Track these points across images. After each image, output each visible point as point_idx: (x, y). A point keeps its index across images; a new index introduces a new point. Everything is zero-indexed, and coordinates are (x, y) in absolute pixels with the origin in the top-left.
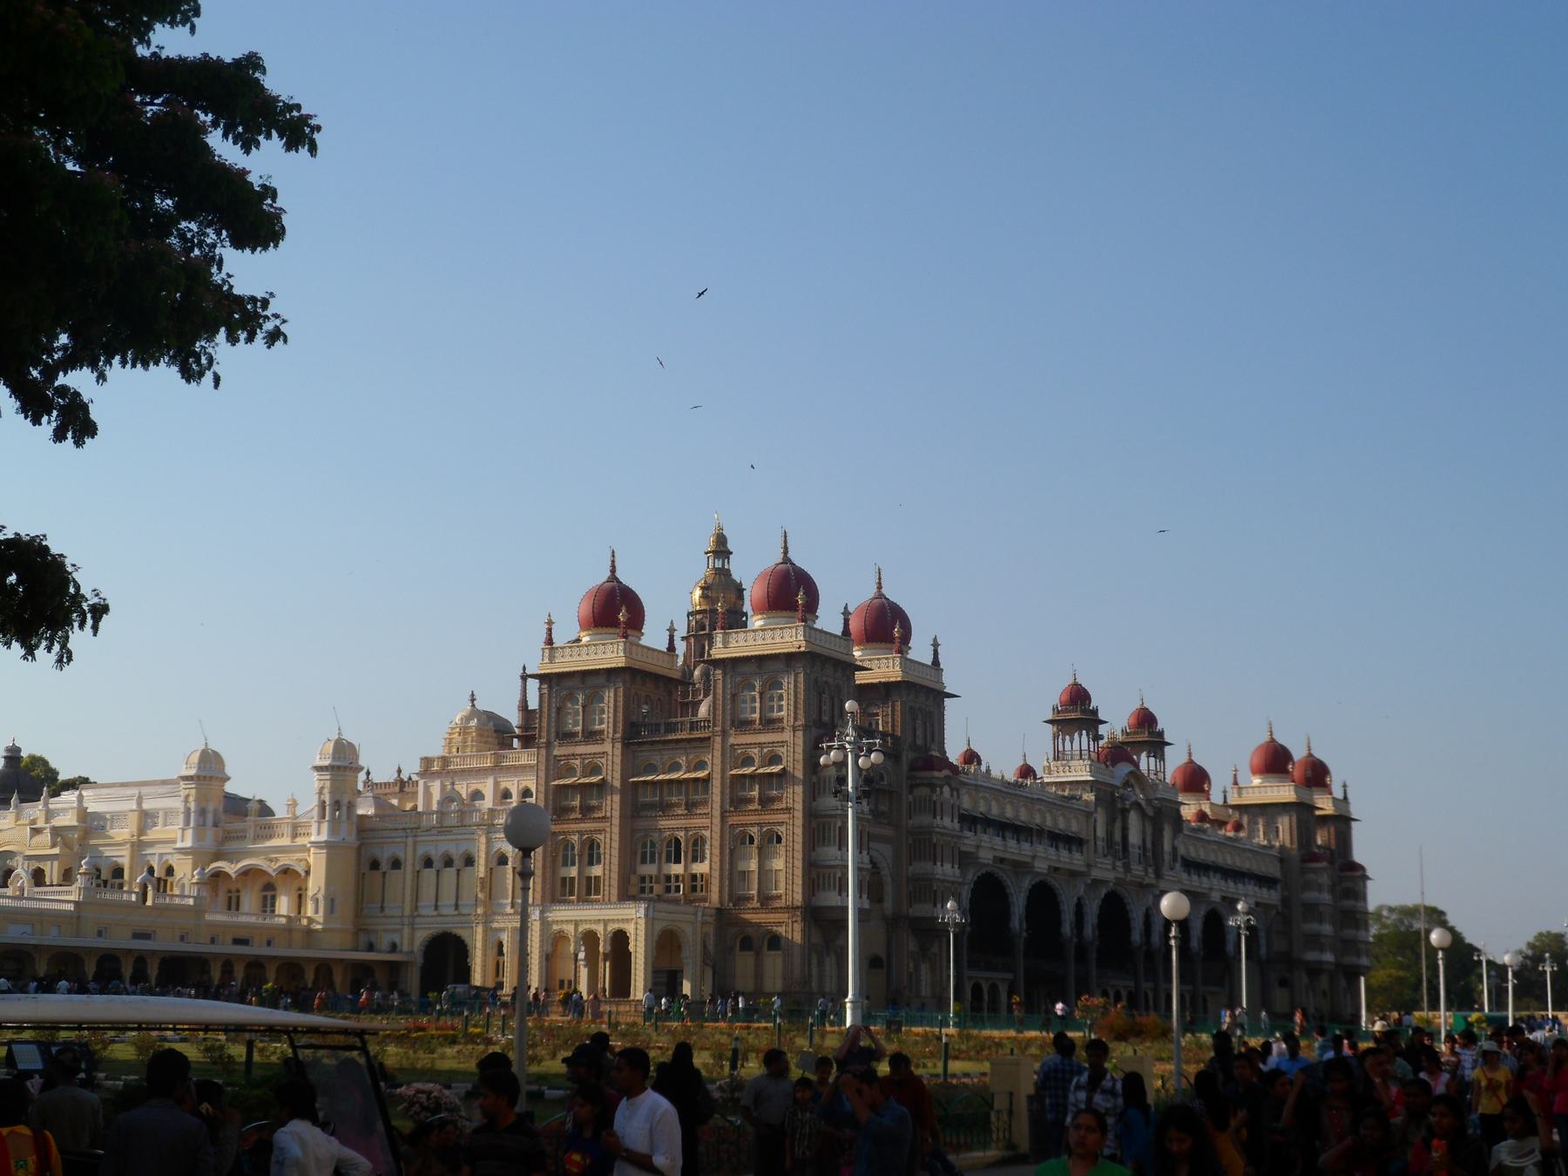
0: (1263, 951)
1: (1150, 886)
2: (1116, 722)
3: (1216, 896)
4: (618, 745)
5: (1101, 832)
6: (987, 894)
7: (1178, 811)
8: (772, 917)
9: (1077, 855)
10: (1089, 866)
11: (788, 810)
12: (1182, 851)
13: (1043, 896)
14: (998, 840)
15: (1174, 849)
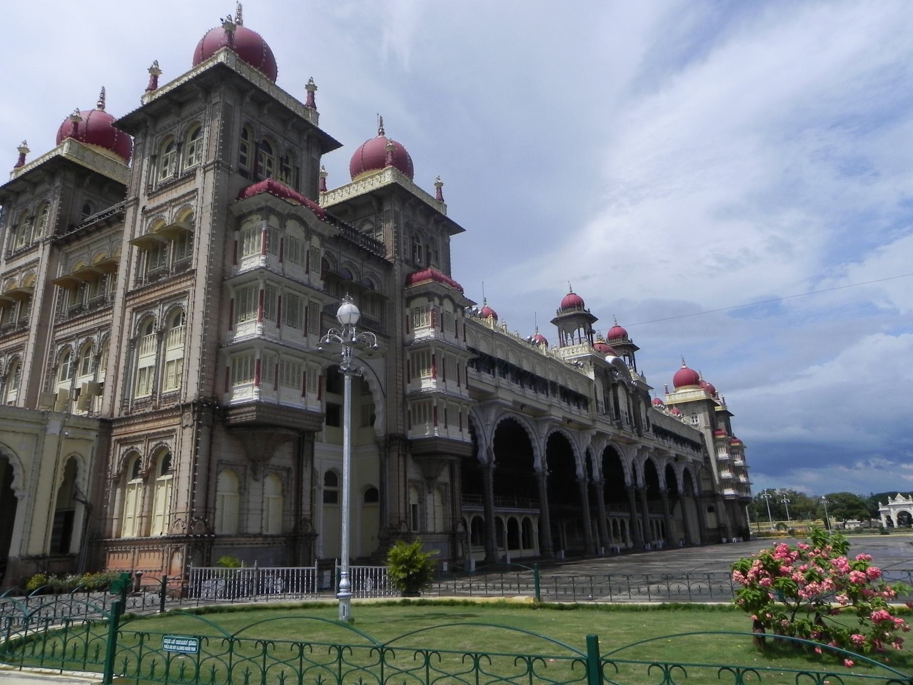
0: (696, 490)
1: (635, 442)
2: (602, 329)
3: (673, 453)
4: (48, 247)
5: (600, 398)
6: (512, 436)
7: (647, 393)
8: (162, 425)
9: (584, 412)
10: (594, 421)
11: (193, 272)
12: (651, 422)
13: (559, 446)
14: (516, 387)
15: (647, 417)
